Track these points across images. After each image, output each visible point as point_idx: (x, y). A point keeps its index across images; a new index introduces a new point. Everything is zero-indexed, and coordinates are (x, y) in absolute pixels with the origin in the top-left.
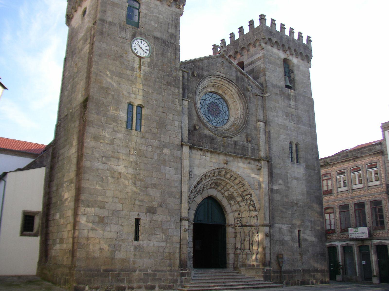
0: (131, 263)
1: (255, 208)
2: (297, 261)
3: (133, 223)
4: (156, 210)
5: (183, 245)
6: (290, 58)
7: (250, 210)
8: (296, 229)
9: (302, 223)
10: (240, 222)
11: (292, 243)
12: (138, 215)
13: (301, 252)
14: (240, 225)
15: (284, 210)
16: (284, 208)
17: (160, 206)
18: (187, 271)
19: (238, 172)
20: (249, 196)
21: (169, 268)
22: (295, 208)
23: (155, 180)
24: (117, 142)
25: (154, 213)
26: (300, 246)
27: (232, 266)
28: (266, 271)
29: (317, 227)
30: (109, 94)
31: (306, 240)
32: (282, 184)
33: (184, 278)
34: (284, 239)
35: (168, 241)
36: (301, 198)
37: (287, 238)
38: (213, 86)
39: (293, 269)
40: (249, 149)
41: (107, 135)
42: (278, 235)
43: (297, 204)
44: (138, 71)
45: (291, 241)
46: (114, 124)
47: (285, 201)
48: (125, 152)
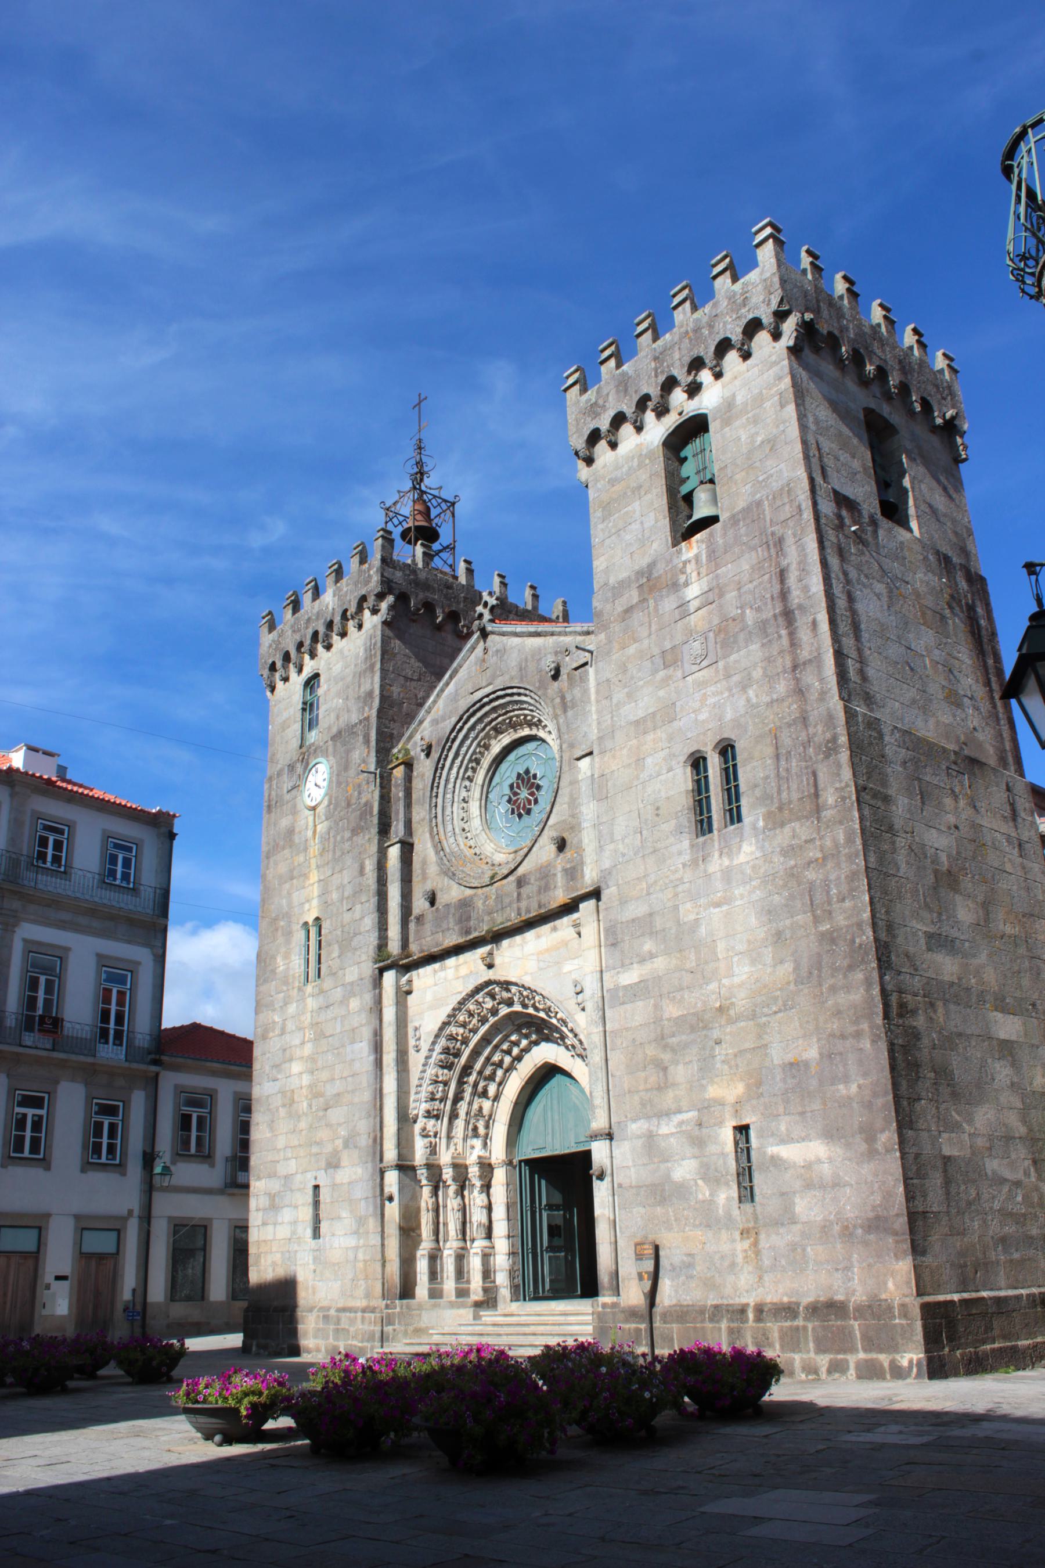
0: (310, 1291)
2: (733, 1265)
3: (309, 1197)
4: (339, 1159)
6: (692, 407)
8: (721, 1123)
9: (748, 1087)
11: (704, 1192)
12: (316, 1178)
13: (751, 1225)
15: (666, 1057)
16: (665, 1047)
17: (346, 1145)
18: (398, 1309)
19: (526, 973)
21: (364, 1303)
22: (716, 1034)
23: (338, 1086)
24: (290, 1026)
25: (337, 1166)
26: (747, 1193)
28: (600, 1309)
29: (841, 1087)
30: (277, 930)
31: (776, 1161)
32: (654, 951)
34: (668, 1177)
35: (361, 1231)
36: (744, 977)
37: (684, 1170)
38: (498, 731)
39: (712, 1300)
40: (559, 875)
41: (277, 1019)
42: (644, 1165)
43: (721, 1009)
44: (312, 843)
45: (700, 1182)
46: (285, 988)
47: (669, 1020)
48: (297, 1042)
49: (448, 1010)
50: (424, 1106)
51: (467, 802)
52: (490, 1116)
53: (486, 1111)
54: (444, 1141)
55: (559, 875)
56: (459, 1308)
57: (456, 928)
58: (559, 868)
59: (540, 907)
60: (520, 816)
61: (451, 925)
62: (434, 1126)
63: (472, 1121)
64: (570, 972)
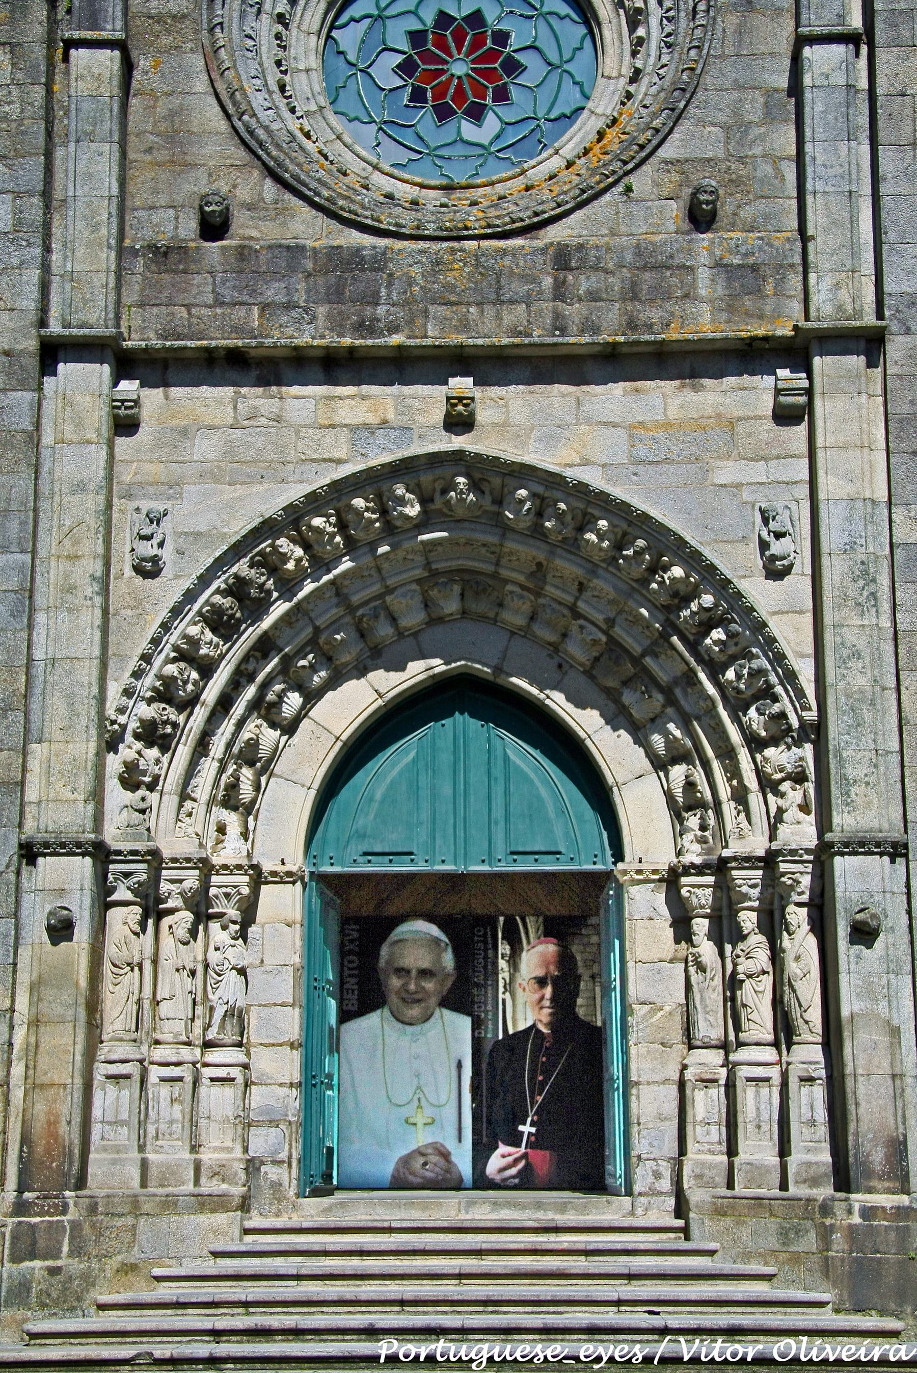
1: (783, 715)
5: (42, 1029)
7: (755, 744)
10: (702, 841)
14: (698, 860)
18: (73, 1214)
20: (718, 634)
27: (657, 1175)
28: (856, 1219)
33: (37, 1264)
40: (703, 274)
49: (295, 492)
50: (146, 711)
51: (286, 26)
52: (270, 761)
53: (264, 750)
54: (171, 801)
55: (703, 274)
56: (213, 1211)
57: (322, 311)
58: (704, 258)
59: (632, 325)
60: (443, 114)
61: (301, 298)
62: (158, 761)
63: (231, 768)
64: (738, 486)
